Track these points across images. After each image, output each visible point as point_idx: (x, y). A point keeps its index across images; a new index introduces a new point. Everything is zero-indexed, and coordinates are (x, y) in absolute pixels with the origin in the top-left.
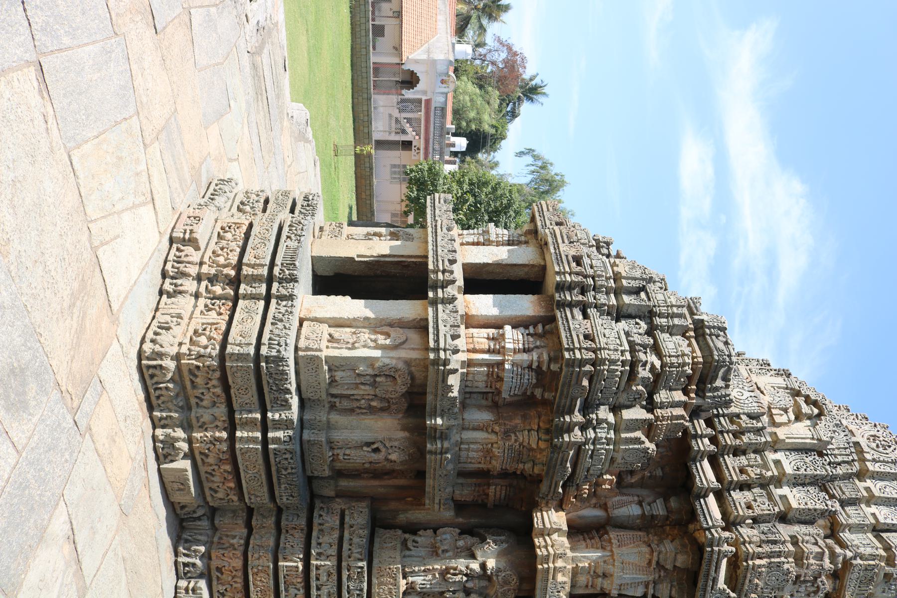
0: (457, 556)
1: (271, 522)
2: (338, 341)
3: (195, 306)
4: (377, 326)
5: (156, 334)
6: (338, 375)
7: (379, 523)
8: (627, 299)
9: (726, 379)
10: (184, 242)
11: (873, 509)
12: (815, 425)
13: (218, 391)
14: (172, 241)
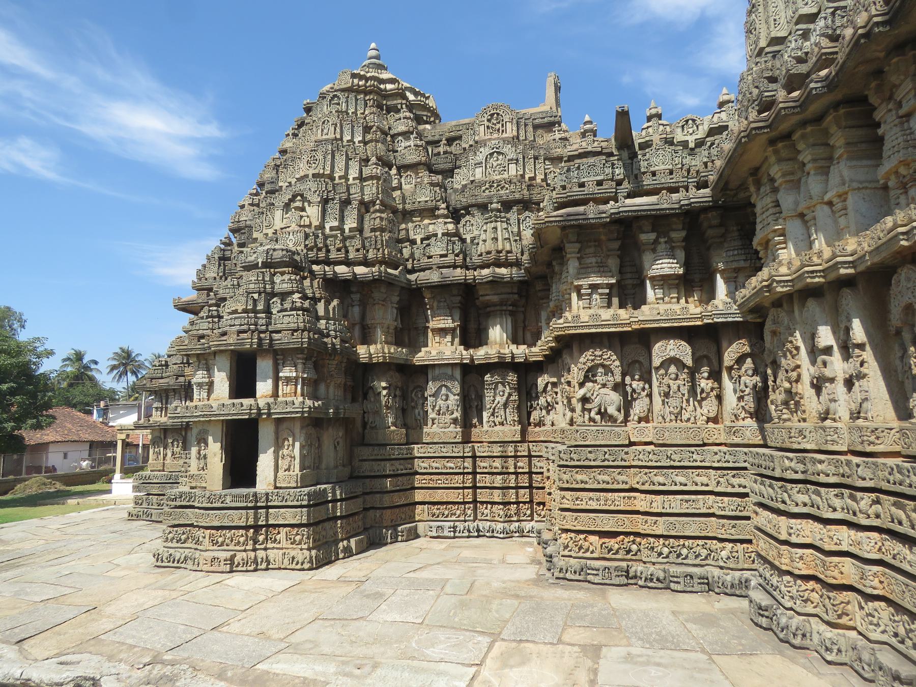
0: (380, 402)
1: (368, 497)
2: (290, 466)
3: (273, 548)
4: (278, 446)
5: (297, 564)
6: (307, 464)
7: (363, 442)
8: (260, 307)
9: (294, 253)
10: (232, 564)
11: (351, 177)
12: (310, 203)
13: (320, 527)
14: (231, 571)
